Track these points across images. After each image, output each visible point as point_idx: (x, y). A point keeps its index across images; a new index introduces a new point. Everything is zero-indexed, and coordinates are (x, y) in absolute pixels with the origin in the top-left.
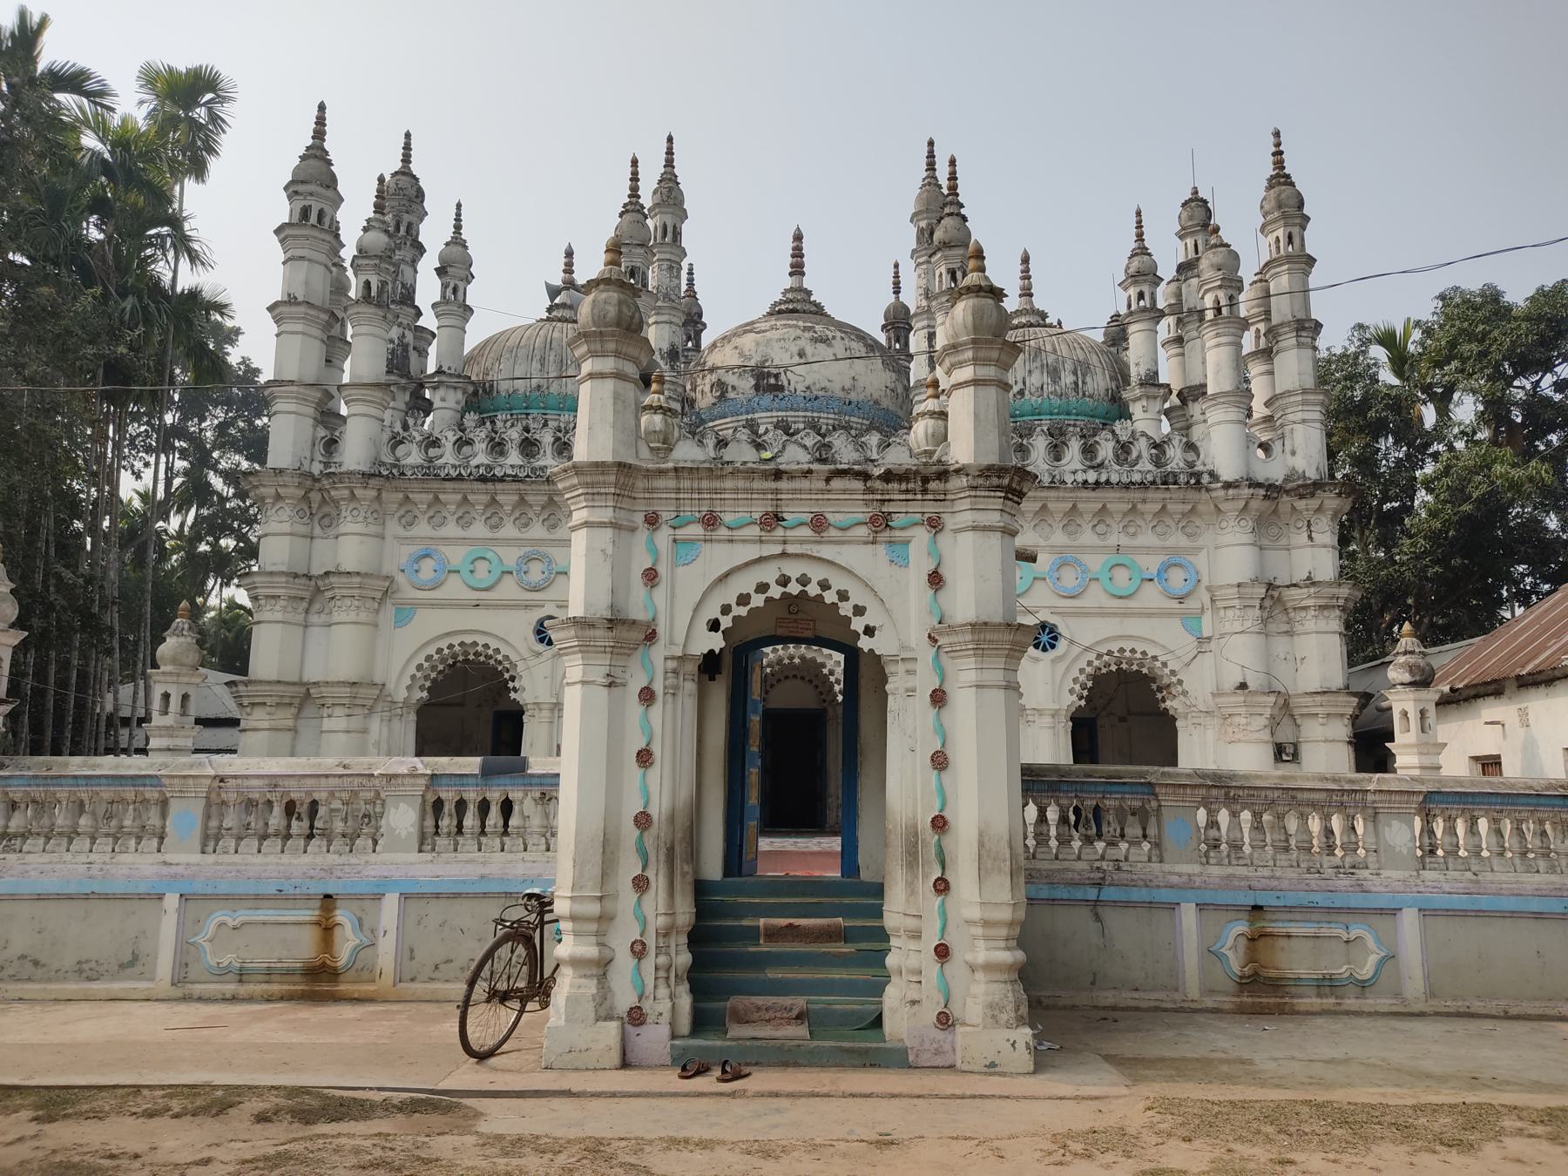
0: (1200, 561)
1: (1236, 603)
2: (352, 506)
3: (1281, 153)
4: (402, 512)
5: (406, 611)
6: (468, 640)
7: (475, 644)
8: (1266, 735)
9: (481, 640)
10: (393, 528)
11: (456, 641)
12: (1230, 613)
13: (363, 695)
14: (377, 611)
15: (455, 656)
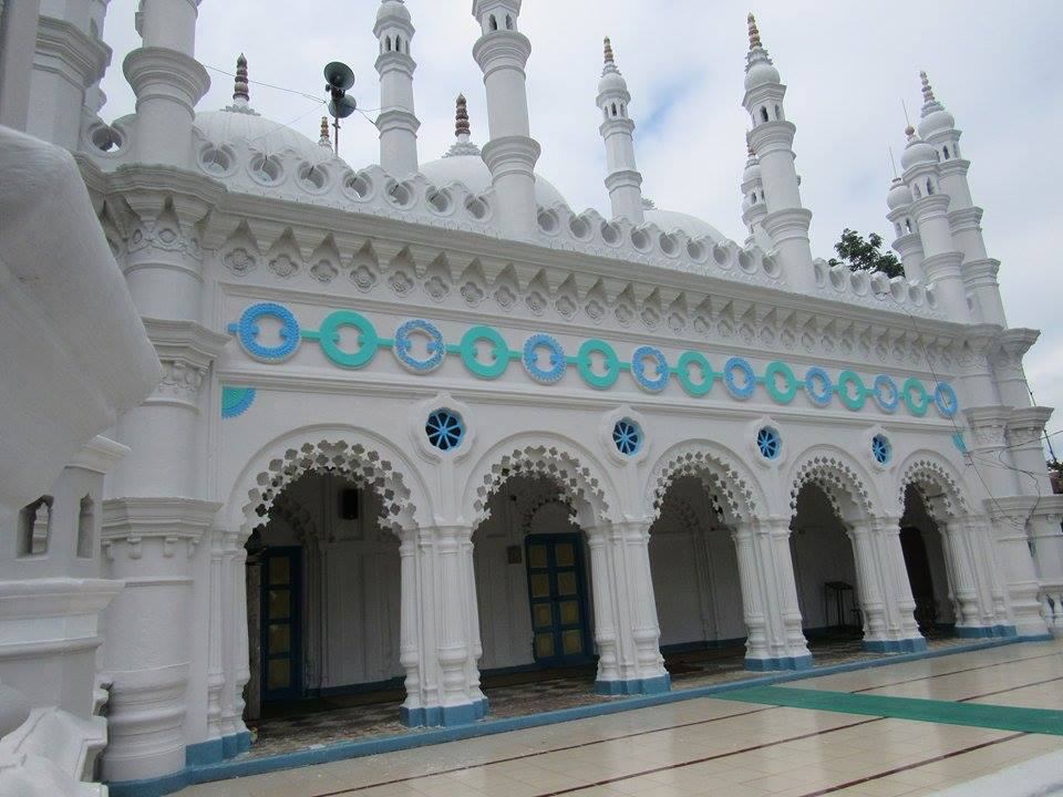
0: (953, 386)
1: (994, 424)
2: (163, 225)
3: (929, 88)
4: (230, 248)
5: (238, 400)
6: (333, 439)
7: (342, 445)
8: (1024, 535)
9: (352, 440)
10: (219, 272)
11: (314, 440)
12: (986, 431)
13: (183, 526)
14: (198, 388)
15: (355, 463)
